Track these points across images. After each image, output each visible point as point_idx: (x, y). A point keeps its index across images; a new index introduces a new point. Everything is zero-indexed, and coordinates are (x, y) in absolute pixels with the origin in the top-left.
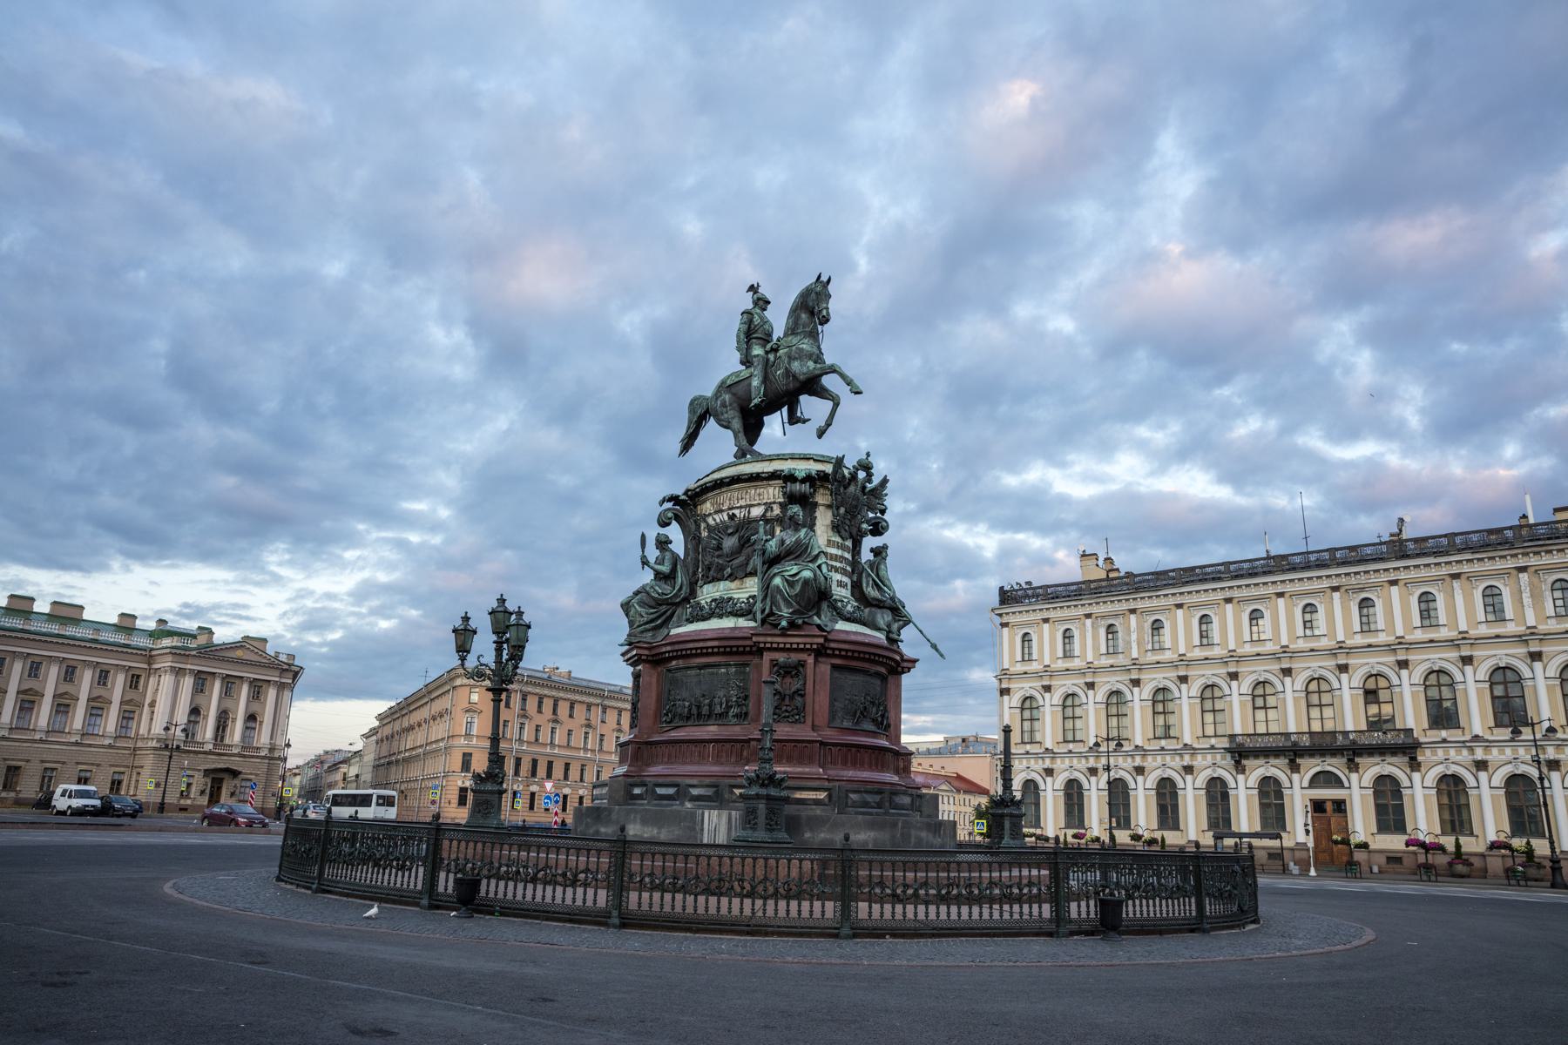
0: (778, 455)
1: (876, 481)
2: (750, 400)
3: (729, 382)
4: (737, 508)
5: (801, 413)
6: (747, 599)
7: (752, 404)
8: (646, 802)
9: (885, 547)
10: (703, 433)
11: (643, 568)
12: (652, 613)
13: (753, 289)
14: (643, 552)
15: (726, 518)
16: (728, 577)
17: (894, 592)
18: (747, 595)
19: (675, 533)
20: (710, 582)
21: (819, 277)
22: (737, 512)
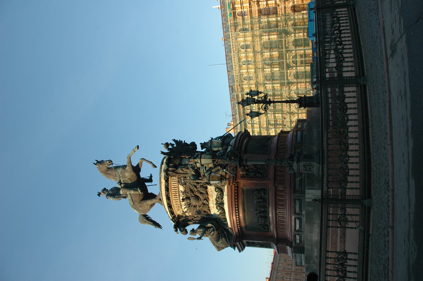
0: (160, 180)
1: (173, 142)
2: (140, 194)
3: (132, 204)
4: (180, 198)
5: (148, 177)
6: (216, 192)
7: (141, 193)
8: (302, 235)
9: (201, 144)
10: (154, 219)
11: (202, 239)
12: (222, 236)
13: (99, 194)
14: (195, 239)
15: (184, 203)
16: (207, 201)
17: (218, 137)
18: (215, 192)
19: (189, 228)
20: (210, 211)
21: (94, 164)
22: (181, 198)
